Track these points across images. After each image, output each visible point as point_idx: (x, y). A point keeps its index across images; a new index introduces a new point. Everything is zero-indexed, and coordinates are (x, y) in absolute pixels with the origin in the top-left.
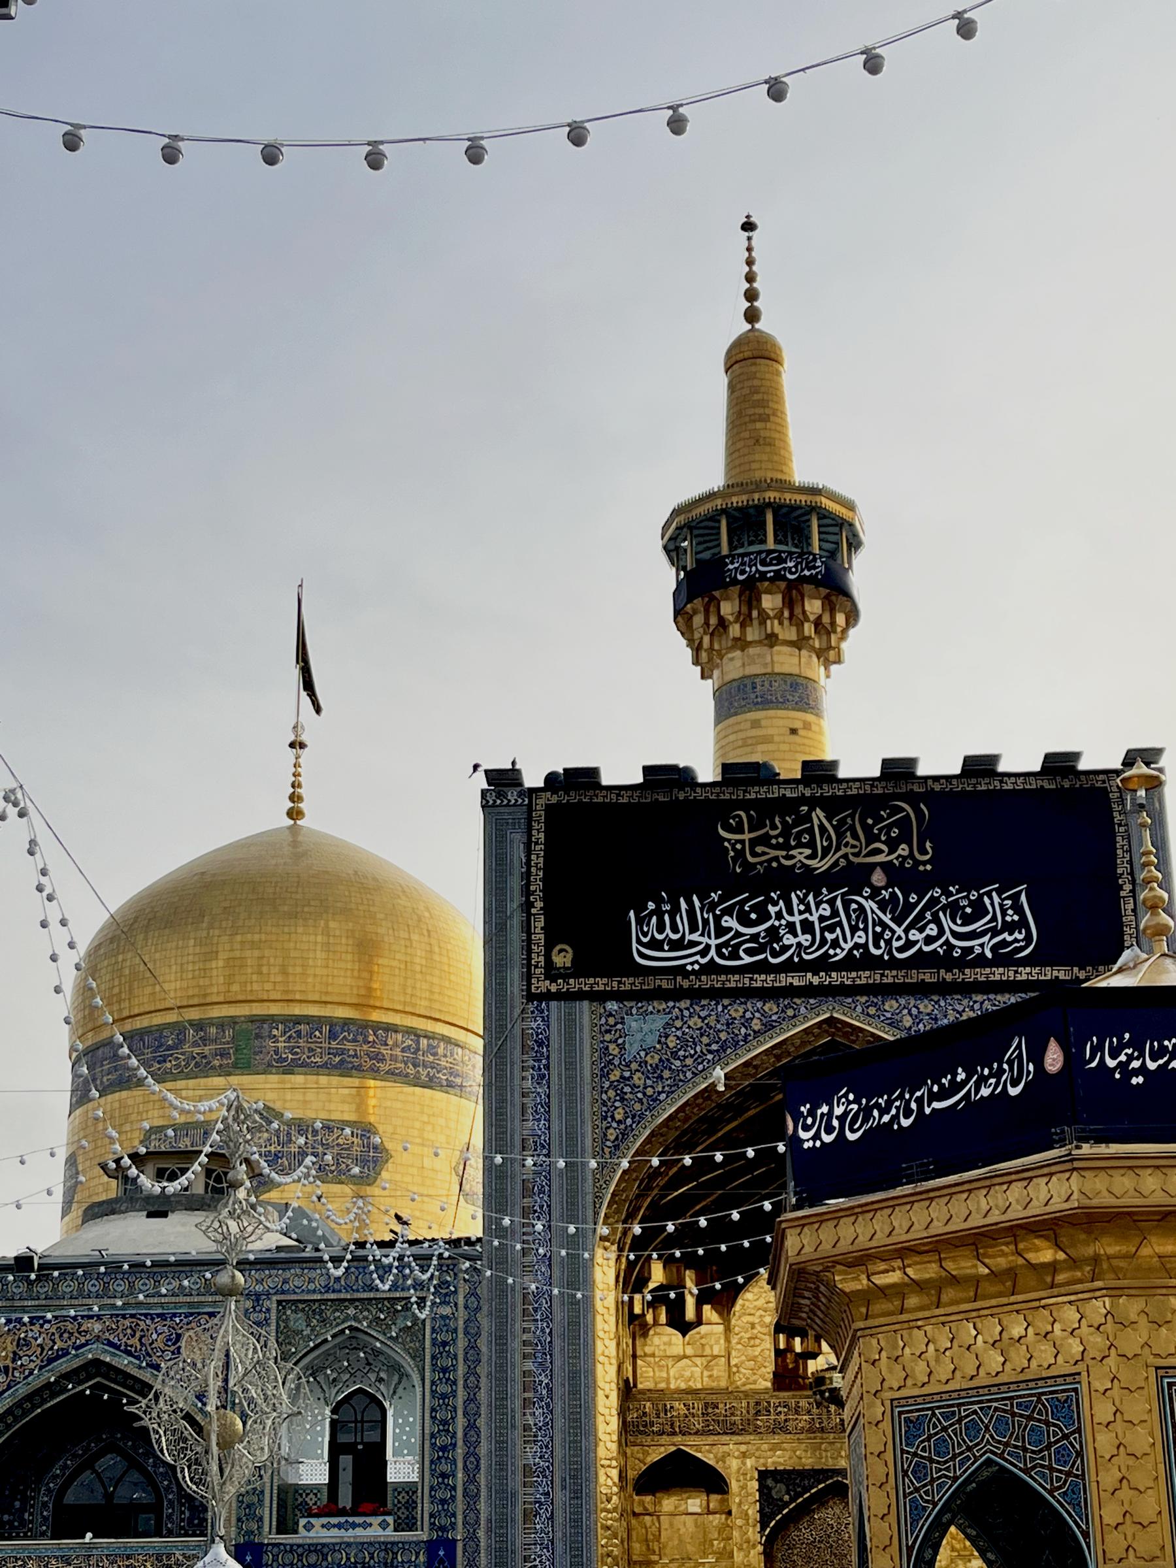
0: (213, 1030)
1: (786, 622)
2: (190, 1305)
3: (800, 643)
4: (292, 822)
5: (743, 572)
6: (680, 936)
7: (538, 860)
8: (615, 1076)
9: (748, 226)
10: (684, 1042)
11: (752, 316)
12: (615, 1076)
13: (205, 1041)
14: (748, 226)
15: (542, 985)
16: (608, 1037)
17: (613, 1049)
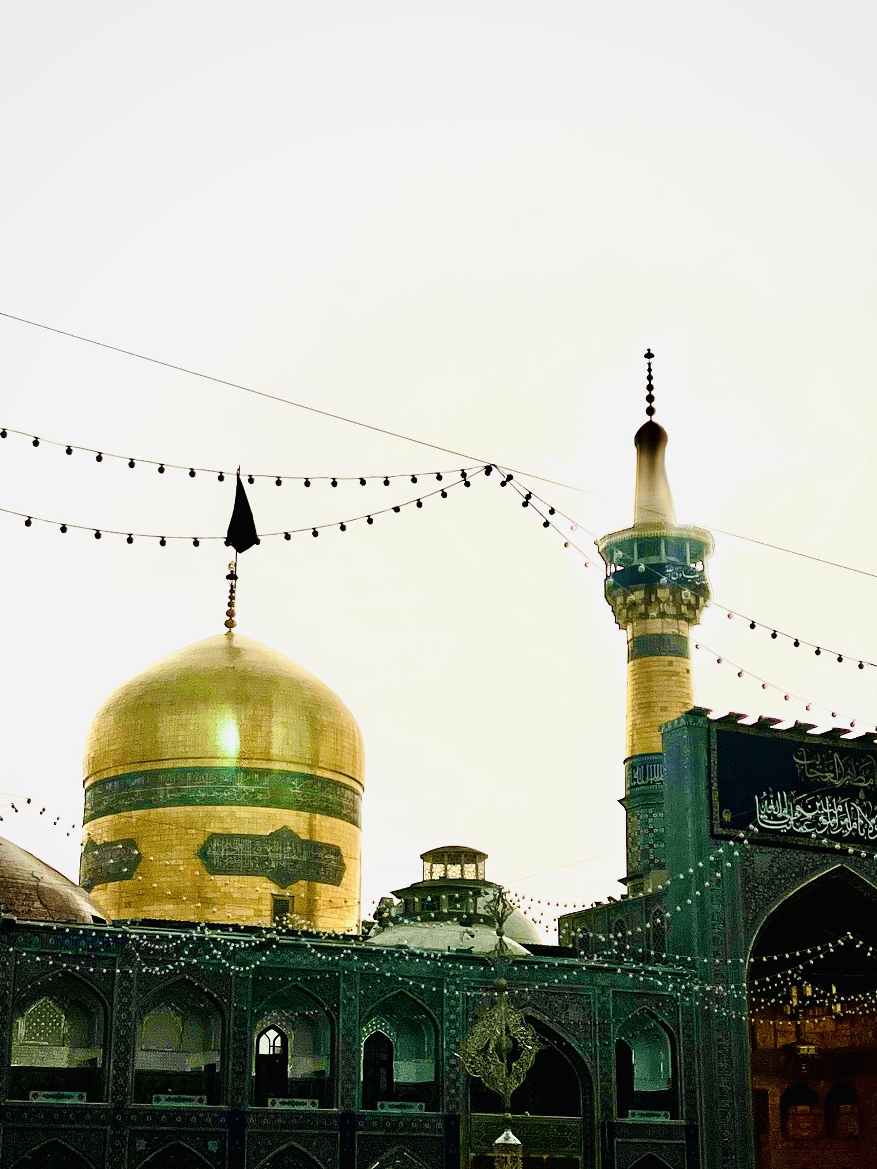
0: (256, 776)
1: (671, 604)
2: (571, 989)
3: (680, 616)
4: (228, 630)
5: (675, 576)
6: (778, 813)
7: (714, 760)
8: (751, 884)
9: (649, 355)
10: (781, 871)
11: (650, 411)
12: (751, 884)
13: (251, 782)
14: (649, 355)
15: (718, 830)
16: (747, 863)
17: (750, 871)
